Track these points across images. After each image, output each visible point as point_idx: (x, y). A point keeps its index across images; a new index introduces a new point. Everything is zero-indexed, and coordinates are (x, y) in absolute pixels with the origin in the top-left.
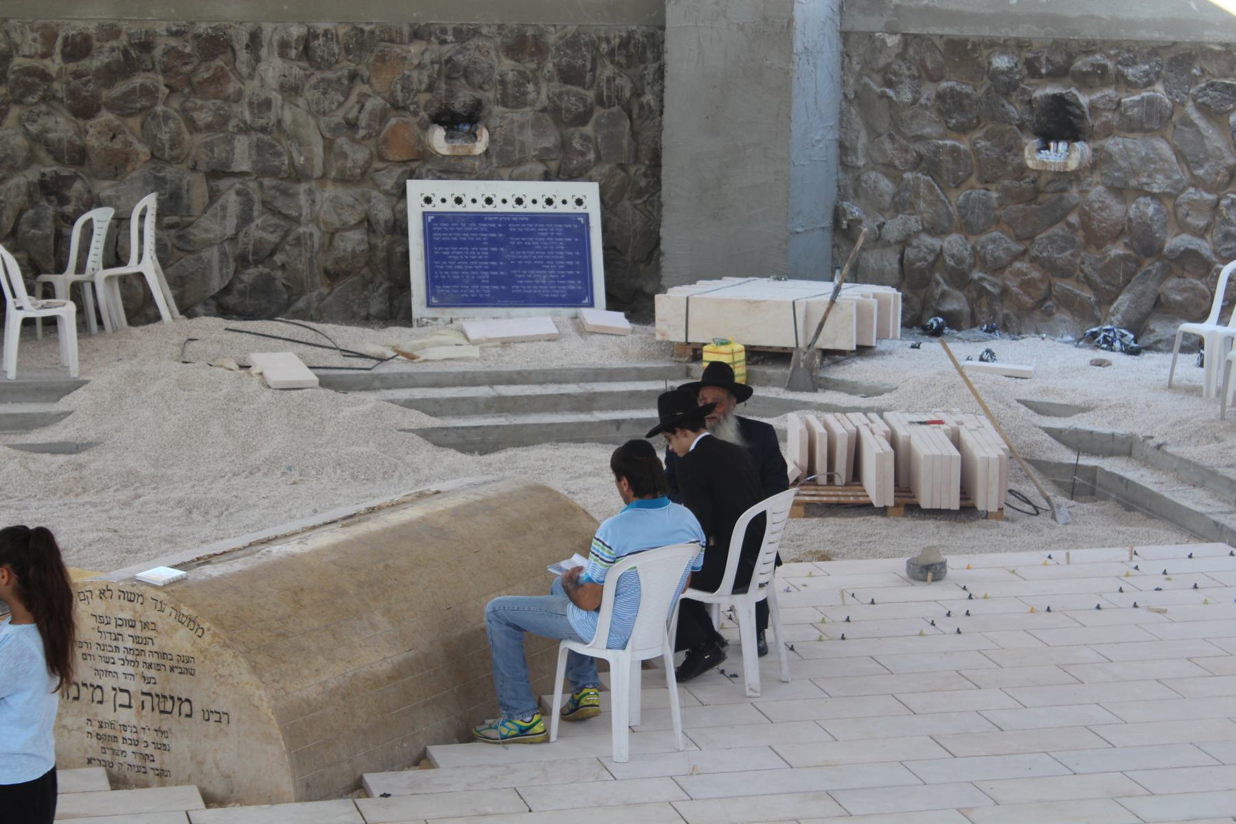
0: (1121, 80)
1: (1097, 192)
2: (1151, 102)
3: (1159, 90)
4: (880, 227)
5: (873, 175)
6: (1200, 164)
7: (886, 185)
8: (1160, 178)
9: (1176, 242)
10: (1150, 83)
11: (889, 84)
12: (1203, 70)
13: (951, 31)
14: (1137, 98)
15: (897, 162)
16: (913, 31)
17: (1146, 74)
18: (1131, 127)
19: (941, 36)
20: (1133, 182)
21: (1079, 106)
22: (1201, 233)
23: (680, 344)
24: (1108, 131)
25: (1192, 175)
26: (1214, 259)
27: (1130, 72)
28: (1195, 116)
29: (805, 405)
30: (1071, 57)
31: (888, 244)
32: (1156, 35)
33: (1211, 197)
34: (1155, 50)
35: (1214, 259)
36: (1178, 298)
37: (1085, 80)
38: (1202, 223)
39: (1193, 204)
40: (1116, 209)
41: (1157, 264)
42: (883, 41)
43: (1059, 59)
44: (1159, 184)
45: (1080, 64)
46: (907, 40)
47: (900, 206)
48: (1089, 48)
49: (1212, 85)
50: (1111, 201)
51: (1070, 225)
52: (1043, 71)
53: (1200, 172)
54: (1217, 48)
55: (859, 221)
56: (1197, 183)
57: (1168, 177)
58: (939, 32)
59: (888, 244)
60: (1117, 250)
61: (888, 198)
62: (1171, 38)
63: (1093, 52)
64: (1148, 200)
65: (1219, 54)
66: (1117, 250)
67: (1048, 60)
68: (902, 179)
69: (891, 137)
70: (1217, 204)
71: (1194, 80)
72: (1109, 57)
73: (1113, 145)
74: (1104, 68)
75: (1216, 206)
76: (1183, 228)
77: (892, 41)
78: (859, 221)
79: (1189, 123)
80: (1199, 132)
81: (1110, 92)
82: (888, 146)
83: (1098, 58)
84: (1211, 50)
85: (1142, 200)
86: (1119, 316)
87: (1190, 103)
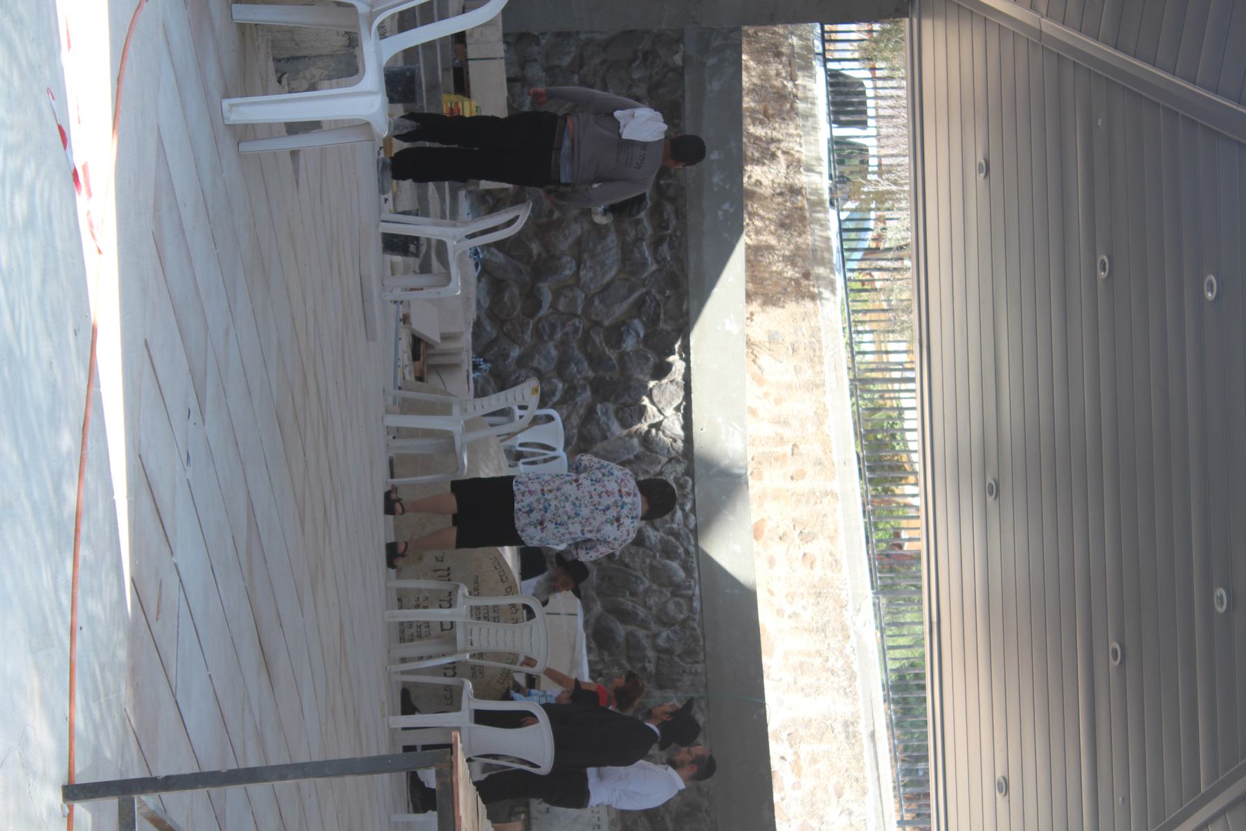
0: (657, 243)
1: (576, 230)
2: (644, 265)
3: (654, 267)
4: (535, 60)
5: (574, 49)
6: (602, 301)
7: (566, 61)
8: (591, 274)
9: (546, 291)
10: (658, 262)
11: (645, 58)
12: (668, 298)
13: (688, 108)
14: (647, 254)
15: (585, 69)
16: (687, 78)
17: (664, 259)
18: (626, 252)
19: (683, 97)
20: (585, 256)
21: (638, 213)
22: (553, 305)
23: (465, 54)
24: (621, 233)
25: (594, 295)
26: (536, 318)
27: (665, 248)
28: (636, 295)
29: (443, 200)
30: (673, 200)
31: (523, 68)
32: (692, 265)
33: (579, 312)
34: (681, 261)
35: (536, 318)
36: (506, 298)
37: (656, 212)
38: (561, 308)
39: (574, 300)
40: (564, 244)
41: (528, 279)
42: (677, 52)
43: (671, 192)
44: (585, 275)
45: (669, 208)
46: (680, 72)
47: (550, 70)
48: (680, 214)
49: (659, 305)
50: (571, 240)
51: (551, 213)
52: (662, 182)
53: (597, 302)
54: (685, 307)
55: (538, 44)
56: (589, 301)
57: (591, 280)
58: (687, 99)
59: (523, 68)
60: (535, 248)
61: (557, 63)
62: (691, 276)
63: (677, 217)
64: (574, 269)
65: (680, 306)
66: (535, 248)
67: (669, 185)
68: (573, 73)
69: (603, 62)
70: (575, 315)
71: (662, 292)
72: (675, 231)
73: (612, 239)
74: (667, 228)
75: (575, 315)
76: (557, 294)
77: (678, 59)
78: (538, 44)
79: (630, 292)
80: (625, 298)
81: (650, 231)
82: (597, 61)
83: (673, 223)
84: (682, 303)
85: (574, 263)
86: (488, 256)
87: (644, 290)
